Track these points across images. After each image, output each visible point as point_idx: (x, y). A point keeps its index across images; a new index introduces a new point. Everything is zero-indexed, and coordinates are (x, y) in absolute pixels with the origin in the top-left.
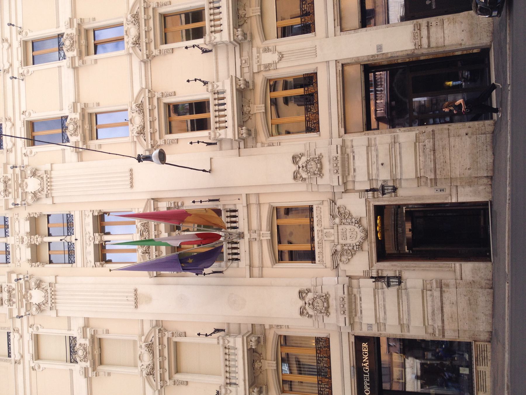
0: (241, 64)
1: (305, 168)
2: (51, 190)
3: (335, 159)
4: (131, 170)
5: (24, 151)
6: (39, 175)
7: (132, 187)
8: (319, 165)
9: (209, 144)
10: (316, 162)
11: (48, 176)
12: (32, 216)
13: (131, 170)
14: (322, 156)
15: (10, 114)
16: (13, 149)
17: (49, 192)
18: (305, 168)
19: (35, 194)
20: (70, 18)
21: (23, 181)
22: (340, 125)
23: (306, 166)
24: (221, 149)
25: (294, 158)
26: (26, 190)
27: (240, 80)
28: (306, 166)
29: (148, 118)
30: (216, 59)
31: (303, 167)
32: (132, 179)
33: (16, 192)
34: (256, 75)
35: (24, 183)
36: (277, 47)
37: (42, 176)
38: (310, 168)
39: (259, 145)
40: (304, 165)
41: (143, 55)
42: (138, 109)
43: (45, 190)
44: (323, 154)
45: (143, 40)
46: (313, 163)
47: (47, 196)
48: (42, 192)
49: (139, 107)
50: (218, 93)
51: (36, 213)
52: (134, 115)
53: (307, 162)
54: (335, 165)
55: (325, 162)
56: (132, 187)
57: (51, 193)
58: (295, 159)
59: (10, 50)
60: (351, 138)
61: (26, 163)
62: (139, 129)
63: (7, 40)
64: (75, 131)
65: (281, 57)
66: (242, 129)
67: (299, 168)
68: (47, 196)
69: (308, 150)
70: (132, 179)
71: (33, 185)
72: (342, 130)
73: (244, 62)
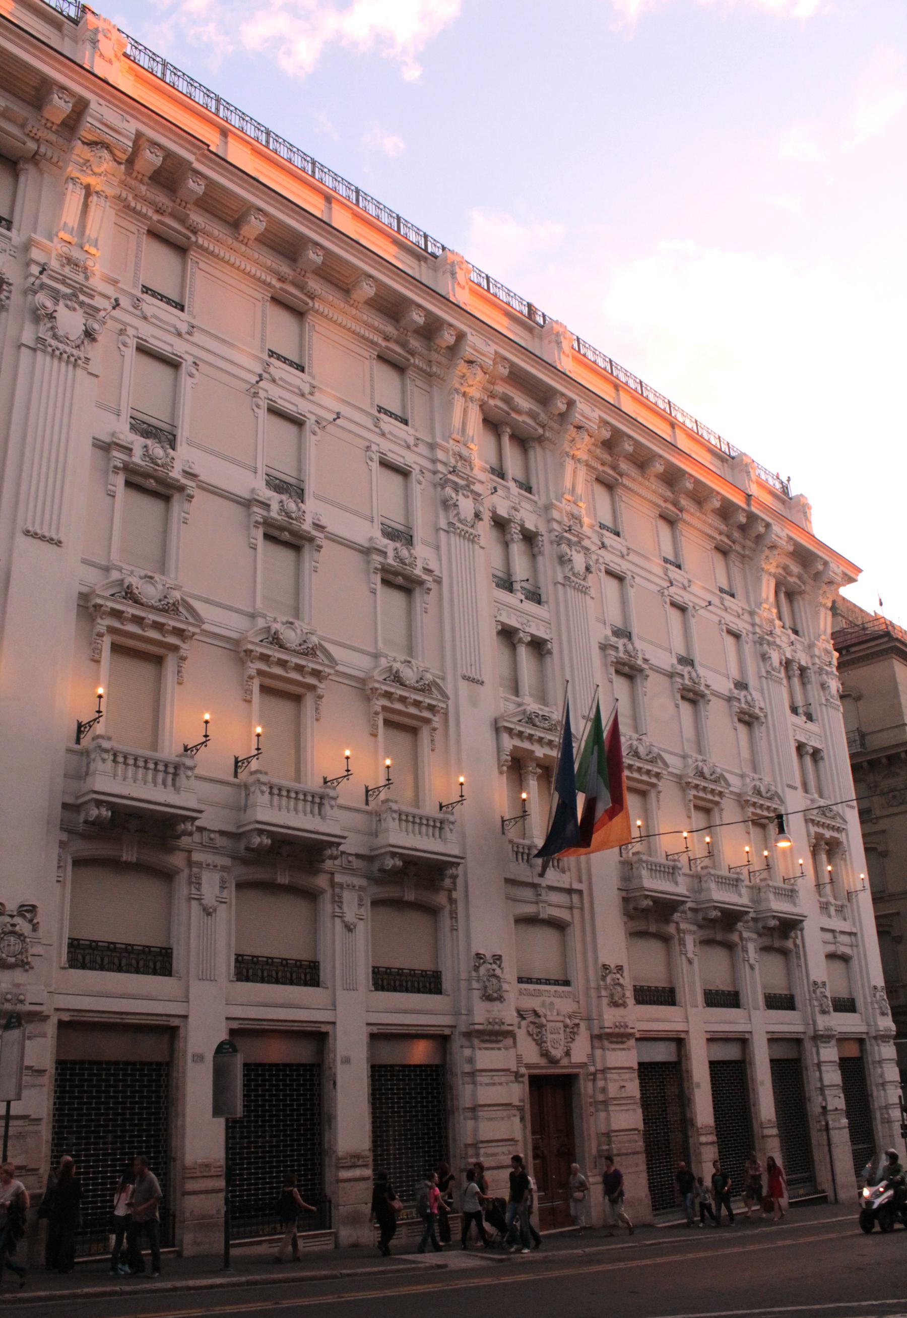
0: (209, 830)
1: (11, 928)
2: (53, 355)
3: (22, 997)
4: (59, 543)
5: (131, 332)
6: (86, 342)
7: (27, 533)
8: (13, 960)
9: (81, 728)
10: (19, 956)
11: (80, 362)
12: (5, 287)
13: (59, 543)
14: (26, 971)
15: (197, 337)
16: (138, 312)
17: (50, 349)
18: (11, 928)
19: (51, 317)
20: (323, 527)
21: (82, 304)
22: (76, 1014)
23: (13, 933)
24: (69, 750)
25: (33, 909)
26: (61, 303)
27: (192, 825)
28: (13, 933)
29: (152, 617)
30: (222, 782)
31: (13, 925)
32: (42, 538)
33: (61, 277)
34: (185, 854)
35: (77, 306)
36: (224, 905)
37: (82, 348)
38: (9, 941)
39: (64, 837)
40: (17, 928)
41: (253, 643)
42: (171, 601)
43: (54, 343)
44: (31, 972)
45: (277, 654)
46: (18, 947)
47: (39, 339)
48: (50, 333)
49: (174, 604)
50: (175, 775)
51: (8, 298)
52: (160, 587)
53: (21, 936)
54: (9, 997)
55: (18, 976)
56: (27, 533)
57: (44, 351)
58: (28, 910)
59: (297, 391)
60: (49, 1035)
61: (110, 323)
62: (136, 591)
63: (312, 394)
64: (151, 459)
65: (208, 912)
66: (107, 810)
67: (12, 916)
68: (39, 339)
69: (43, 941)
70: (42, 538)
71: (71, 321)
72: (66, 1017)
73: (212, 836)
